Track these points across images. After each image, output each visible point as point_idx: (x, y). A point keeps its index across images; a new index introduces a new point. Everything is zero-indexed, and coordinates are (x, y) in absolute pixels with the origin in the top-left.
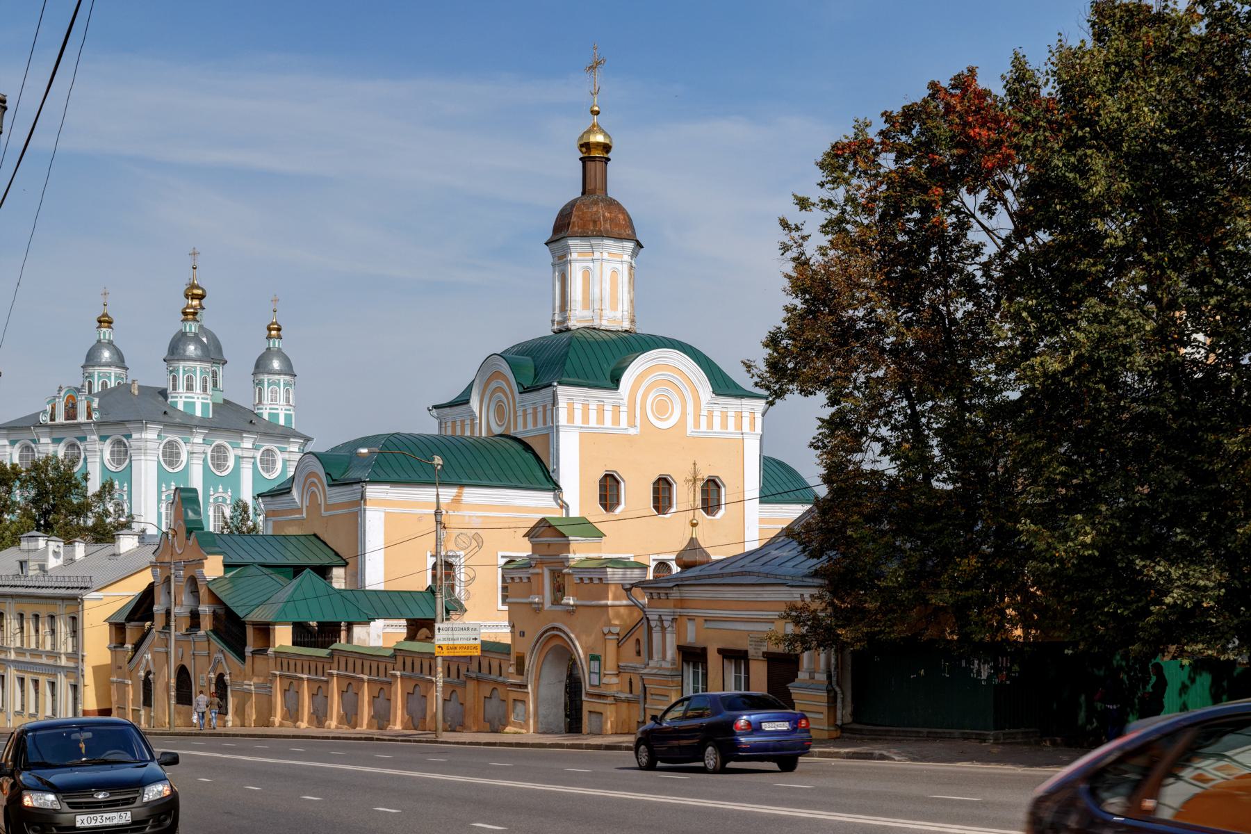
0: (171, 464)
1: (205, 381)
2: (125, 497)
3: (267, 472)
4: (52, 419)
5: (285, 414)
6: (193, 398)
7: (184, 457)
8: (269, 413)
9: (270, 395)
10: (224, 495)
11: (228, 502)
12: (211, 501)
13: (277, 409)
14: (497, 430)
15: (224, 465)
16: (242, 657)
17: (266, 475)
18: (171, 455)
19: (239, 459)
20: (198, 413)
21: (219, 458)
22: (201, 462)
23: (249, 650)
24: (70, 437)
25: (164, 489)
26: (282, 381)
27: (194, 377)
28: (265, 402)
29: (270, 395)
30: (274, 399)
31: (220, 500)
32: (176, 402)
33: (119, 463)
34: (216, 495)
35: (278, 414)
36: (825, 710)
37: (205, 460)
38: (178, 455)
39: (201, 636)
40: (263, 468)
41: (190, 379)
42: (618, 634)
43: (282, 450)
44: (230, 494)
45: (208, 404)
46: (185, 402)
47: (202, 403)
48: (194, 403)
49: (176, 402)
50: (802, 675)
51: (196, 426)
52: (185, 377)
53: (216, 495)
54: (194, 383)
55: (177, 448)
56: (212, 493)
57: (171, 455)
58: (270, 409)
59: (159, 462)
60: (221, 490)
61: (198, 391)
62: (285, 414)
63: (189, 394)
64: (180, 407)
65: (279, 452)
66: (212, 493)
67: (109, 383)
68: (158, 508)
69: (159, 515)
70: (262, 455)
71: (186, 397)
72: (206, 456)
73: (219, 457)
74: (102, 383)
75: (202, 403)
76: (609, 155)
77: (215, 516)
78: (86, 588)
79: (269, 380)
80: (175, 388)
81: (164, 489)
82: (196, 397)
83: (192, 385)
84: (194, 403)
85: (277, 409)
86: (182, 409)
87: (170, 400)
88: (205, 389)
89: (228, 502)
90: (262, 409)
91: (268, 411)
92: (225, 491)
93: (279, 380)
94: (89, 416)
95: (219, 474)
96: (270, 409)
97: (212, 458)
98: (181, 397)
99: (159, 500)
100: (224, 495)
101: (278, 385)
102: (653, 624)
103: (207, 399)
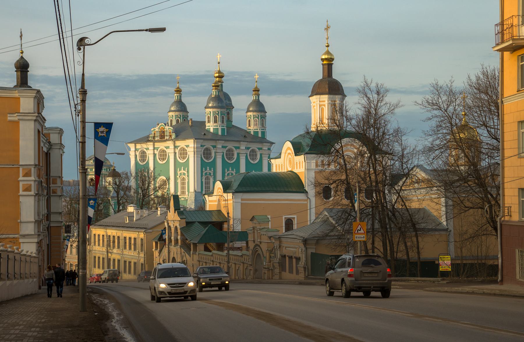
0: (207, 158)
1: (223, 118)
2: (186, 174)
3: (253, 160)
5: (262, 132)
7: (213, 155)
8: (254, 132)
10: (232, 172)
12: (226, 175)
14: (290, 169)
17: (252, 162)
18: (207, 154)
19: (238, 154)
20: (220, 133)
21: (229, 155)
24: (161, 146)
25: (204, 170)
26: (260, 115)
28: (252, 126)
31: (230, 174)
32: (210, 128)
34: (229, 172)
36: (303, 272)
37: (223, 156)
38: (210, 154)
40: (250, 158)
41: (215, 118)
42: (270, 250)
43: (260, 149)
44: (235, 171)
45: (225, 128)
47: (222, 128)
49: (210, 128)
50: (300, 263)
51: (218, 140)
53: (229, 172)
54: (218, 119)
55: (210, 151)
56: (226, 171)
57: (207, 154)
58: (254, 129)
59: (201, 158)
60: (230, 170)
61: (220, 123)
64: (212, 130)
66: (226, 171)
67: (180, 120)
68: (201, 179)
69: (202, 182)
70: (250, 152)
71: (214, 126)
73: (230, 154)
75: (222, 128)
76: (333, 62)
78: (146, 228)
79: (253, 115)
80: (209, 122)
81: (204, 170)
83: (217, 120)
87: (207, 127)
88: (223, 122)
92: (233, 170)
95: (229, 162)
97: (226, 155)
98: (212, 126)
99: (202, 176)
100: (232, 172)
102: (276, 248)
103: (224, 126)
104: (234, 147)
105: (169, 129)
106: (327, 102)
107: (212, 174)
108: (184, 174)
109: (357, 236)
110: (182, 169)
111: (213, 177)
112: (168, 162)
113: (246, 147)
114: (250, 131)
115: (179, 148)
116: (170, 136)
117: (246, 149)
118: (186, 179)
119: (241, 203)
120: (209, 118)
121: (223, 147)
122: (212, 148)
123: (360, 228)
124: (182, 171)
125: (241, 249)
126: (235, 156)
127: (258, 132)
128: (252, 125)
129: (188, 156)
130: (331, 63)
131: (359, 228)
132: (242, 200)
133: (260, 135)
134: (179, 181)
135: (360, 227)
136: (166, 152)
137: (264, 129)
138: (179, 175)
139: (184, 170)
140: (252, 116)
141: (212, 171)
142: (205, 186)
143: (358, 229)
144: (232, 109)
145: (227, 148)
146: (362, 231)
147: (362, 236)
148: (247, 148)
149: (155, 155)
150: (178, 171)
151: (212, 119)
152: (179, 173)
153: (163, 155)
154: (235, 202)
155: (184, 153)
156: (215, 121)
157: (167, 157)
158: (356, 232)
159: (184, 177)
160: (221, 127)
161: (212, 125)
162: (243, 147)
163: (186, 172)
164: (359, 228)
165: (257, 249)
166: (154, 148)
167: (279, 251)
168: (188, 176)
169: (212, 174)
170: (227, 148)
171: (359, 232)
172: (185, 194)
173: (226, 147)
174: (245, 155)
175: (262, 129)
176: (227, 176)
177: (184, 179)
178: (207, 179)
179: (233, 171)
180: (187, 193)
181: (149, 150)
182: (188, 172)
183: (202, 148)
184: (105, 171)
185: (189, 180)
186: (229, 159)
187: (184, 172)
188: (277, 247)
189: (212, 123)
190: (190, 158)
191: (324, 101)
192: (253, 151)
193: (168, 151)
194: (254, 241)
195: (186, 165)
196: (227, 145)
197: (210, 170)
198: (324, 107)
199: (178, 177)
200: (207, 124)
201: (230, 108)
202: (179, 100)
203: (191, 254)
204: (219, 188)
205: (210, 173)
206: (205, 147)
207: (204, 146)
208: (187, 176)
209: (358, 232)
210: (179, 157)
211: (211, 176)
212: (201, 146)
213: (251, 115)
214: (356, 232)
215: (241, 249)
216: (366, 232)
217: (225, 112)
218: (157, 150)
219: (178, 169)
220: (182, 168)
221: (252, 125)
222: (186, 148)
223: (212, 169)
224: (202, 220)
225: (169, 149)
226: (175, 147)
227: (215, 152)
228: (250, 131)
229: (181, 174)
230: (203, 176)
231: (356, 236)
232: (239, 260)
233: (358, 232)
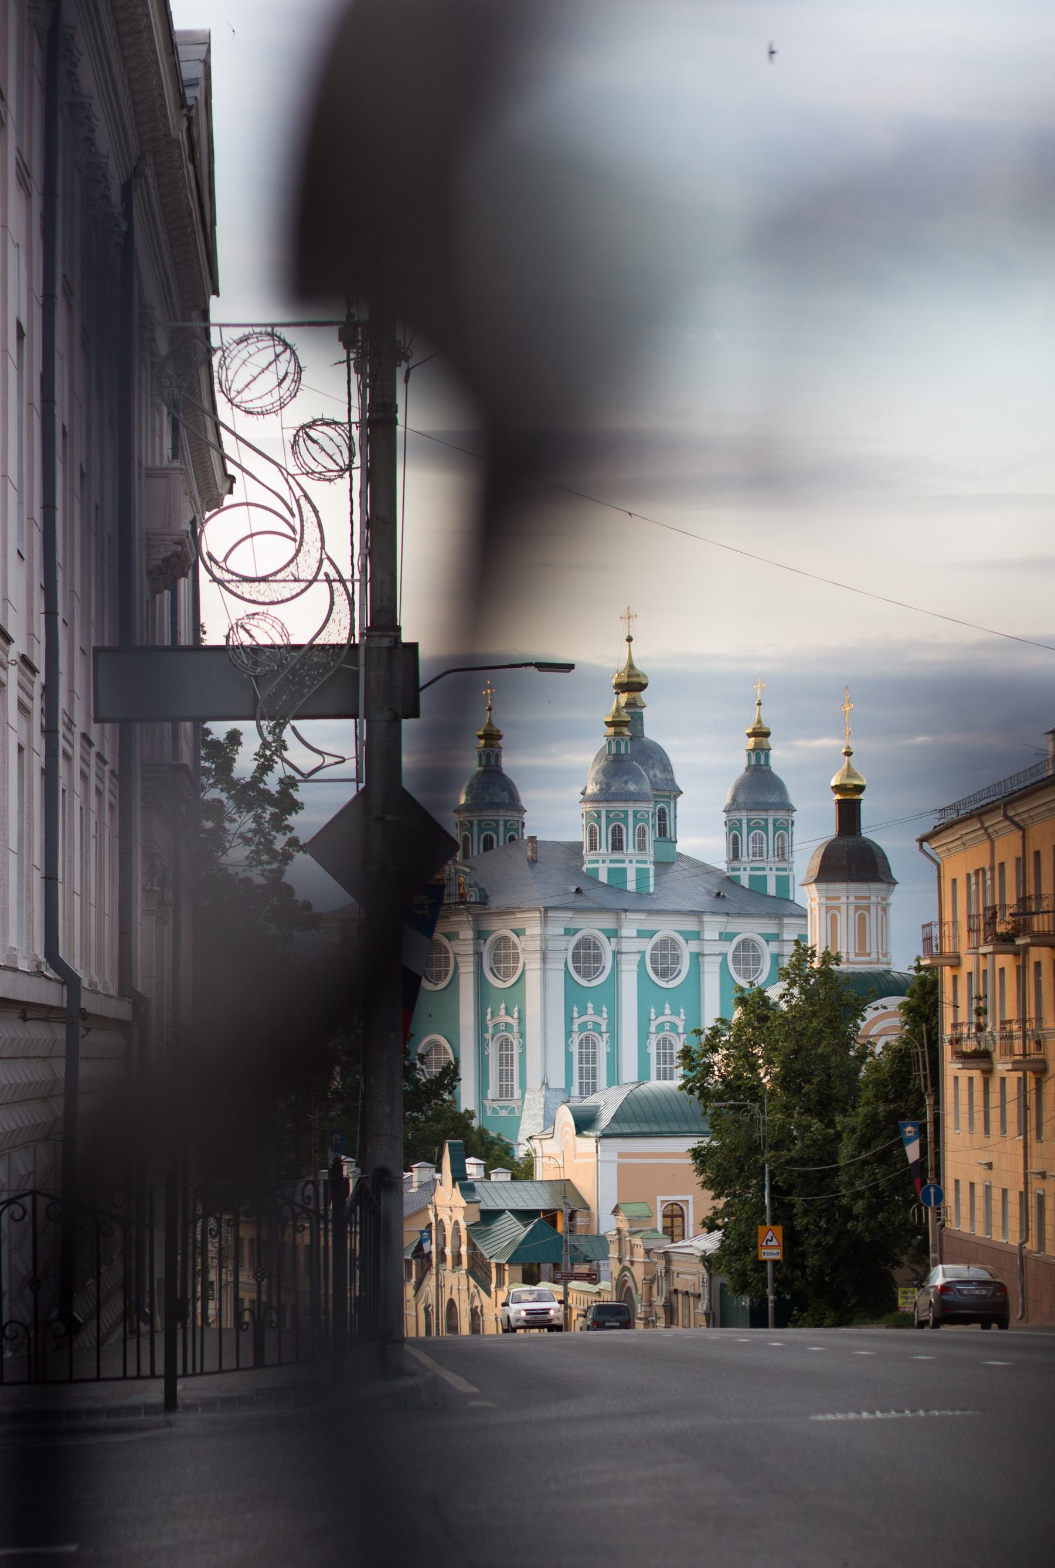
0: (587, 974)
2: (516, 1029)
5: (777, 877)
6: (623, 861)
7: (608, 962)
8: (751, 877)
9: (751, 845)
10: (673, 1019)
12: (653, 1029)
13: (764, 869)
15: (673, 970)
16: (489, 1294)
18: (587, 959)
19: (697, 958)
22: (635, 968)
23: (493, 1285)
25: (576, 1015)
27: (624, 829)
28: (744, 859)
29: (751, 845)
30: (758, 853)
31: (667, 1028)
32: (597, 870)
34: (661, 1019)
35: (765, 877)
37: (641, 964)
38: (598, 958)
39: (462, 1274)
44: (683, 1017)
46: (609, 869)
48: (624, 870)
49: (597, 870)
51: (626, 911)
52: (610, 829)
53: (661, 1019)
55: (596, 947)
56: (653, 1017)
58: (752, 869)
60: (667, 1011)
61: (631, 850)
62: (777, 877)
63: (617, 856)
65: (764, 943)
66: (653, 1017)
67: (495, 838)
69: (569, 1056)
70: (737, 949)
71: (611, 861)
72: (643, 959)
74: (486, 838)
77: (658, 1054)
79: (749, 821)
83: (621, 841)
84: (624, 871)
85: (764, 869)
86: (606, 882)
89: (681, 1030)
90: (738, 869)
91: (748, 872)
92: (675, 1012)
93: (766, 821)
95: (662, 983)
96: (752, 869)
97: (653, 960)
98: (604, 862)
99: (569, 1033)
100: (673, 1019)
101: (765, 829)
103: (645, 862)
104: (681, 933)
106: (843, 900)
107: (604, 1029)
109: (766, 1251)
110: (503, 1012)
111: (606, 1036)
113: (721, 934)
114: (739, 877)
117: (720, 940)
118: (515, 1043)
119: (619, 1165)
121: (642, 934)
122: (603, 937)
123: (772, 1237)
125: (594, 1277)
126: (685, 966)
127: (765, 877)
129: (520, 965)
130: (856, 797)
131: (769, 1237)
132: (621, 1155)
133: (772, 890)
135: (770, 1234)
137: (785, 869)
140: (744, 821)
141: (605, 1015)
142: (581, 1069)
143: (767, 1238)
144: (675, 797)
145: (656, 938)
146: (775, 1243)
147: (775, 1251)
148: (726, 937)
150: (489, 1017)
151: (605, 837)
152: (490, 1024)
154: (602, 1161)
157: (451, 969)
158: (764, 1244)
159: (510, 1036)
160: (635, 865)
162: (711, 933)
163: (514, 1022)
164: (769, 1237)
165: (625, 1278)
167: (666, 1280)
168: (522, 1035)
169: (604, 1029)
170: (656, 938)
171: (769, 1243)
172: (512, 1094)
173: (651, 934)
174: (720, 959)
175: (778, 869)
176: (657, 1033)
177: (505, 1044)
178: (587, 1043)
179: (678, 1014)
180: (517, 1093)
182: (521, 1020)
183: (567, 938)
185: (523, 1047)
186: (664, 974)
187: (509, 1019)
188: (661, 1272)
189: (604, 850)
190: (527, 973)
191: (838, 898)
192: (747, 945)
194: (620, 1260)
196: (656, 929)
197: (598, 1012)
198: (837, 914)
199: (488, 1036)
200: (588, 855)
201: (669, 797)
203: (493, 1289)
204: (566, 1123)
205: (597, 1025)
206: (578, 936)
207: (577, 931)
208: (517, 1036)
209: (767, 1243)
210: (491, 969)
211: (601, 1034)
213: (740, 821)
214: (764, 1244)
215: (594, 1277)
216: (781, 1245)
217: (647, 812)
220: (503, 1006)
222: (513, 937)
223: (605, 1009)
224: (522, 1206)
227: (614, 952)
228: (739, 877)
229: (496, 1026)
230: (573, 1034)
231: (763, 1251)
232: (586, 1301)
233: (767, 1243)
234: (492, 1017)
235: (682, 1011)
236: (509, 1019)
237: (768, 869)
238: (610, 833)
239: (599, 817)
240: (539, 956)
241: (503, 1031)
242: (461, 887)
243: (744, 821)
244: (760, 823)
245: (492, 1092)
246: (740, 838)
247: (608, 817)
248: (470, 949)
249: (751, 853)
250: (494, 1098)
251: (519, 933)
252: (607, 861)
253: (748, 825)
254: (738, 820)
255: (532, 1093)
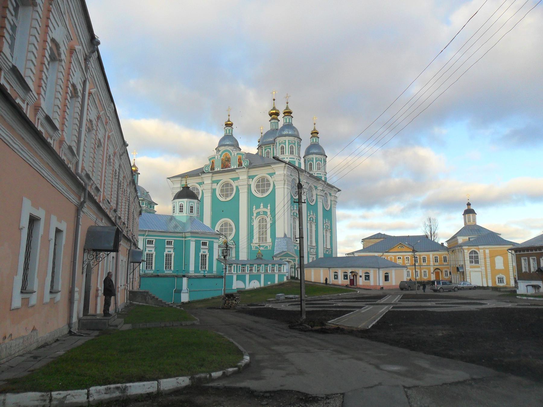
2: (269, 213)
4: (212, 168)
11: (314, 221)
13: (321, 174)
17: (326, 208)
24: (225, 178)
26: (322, 159)
28: (315, 170)
31: (311, 220)
33: (263, 192)
34: (311, 216)
41: (292, 148)
52: (289, 146)
54: (294, 150)
61: (296, 155)
63: (292, 156)
71: (290, 158)
79: (316, 158)
82: (295, 158)
84: (295, 161)
85: (321, 174)
89: (314, 221)
94: (240, 164)
98: (287, 158)
101: (321, 161)
105: (238, 154)
108: (265, 213)
110: (262, 207)
112: (237, 198)
115: (255, 178)
116: (240, 164)
120: (282, 148)
124: (262, 209)
128: (315, 168)
134: (256, 223)
136: (231, 185)
138: (255, 215)
139: (265, 206)
140: (314, 158)
149: (214, 191)
150: (254, 209)
153: (227, 188)
155: (263, 184)
156: (292, 153)
161: (287, 157)
166: (213, 182)
172: (266, 240)
177: (263, 220)
181: (204, 184)
184: (147, 207)
187: (265, 210)
189: (287, 154)
193: (234, 184)
195: (271, 200)
202: (231, 134)
210: (255, 190)
212: (291, 175)
218: (217, 184)
219: (254, 207)
220: (262, 204)
221: (315, 168)
225: (239, 180)
226: (251, 177)
229: (258, 214)
234: (256, 209)
235: (314, 214)
236: (265, 210)
237: (322, 174)
238: (289, 148)
239: (285, 142)
240: (283, 182)
241: (262, 215)
242: (240, 160)
243: (314, 158)
244: (319, 159)
245: (256, 240)
246: (313, 164)
247: (289, 142)
248: (246, 183)
249: (317, 169)
250: (256, 243)
251: (271, 175)
252: (289, 158)
253: (316, 160)
254: (312, 158)
255: (279, 239)
